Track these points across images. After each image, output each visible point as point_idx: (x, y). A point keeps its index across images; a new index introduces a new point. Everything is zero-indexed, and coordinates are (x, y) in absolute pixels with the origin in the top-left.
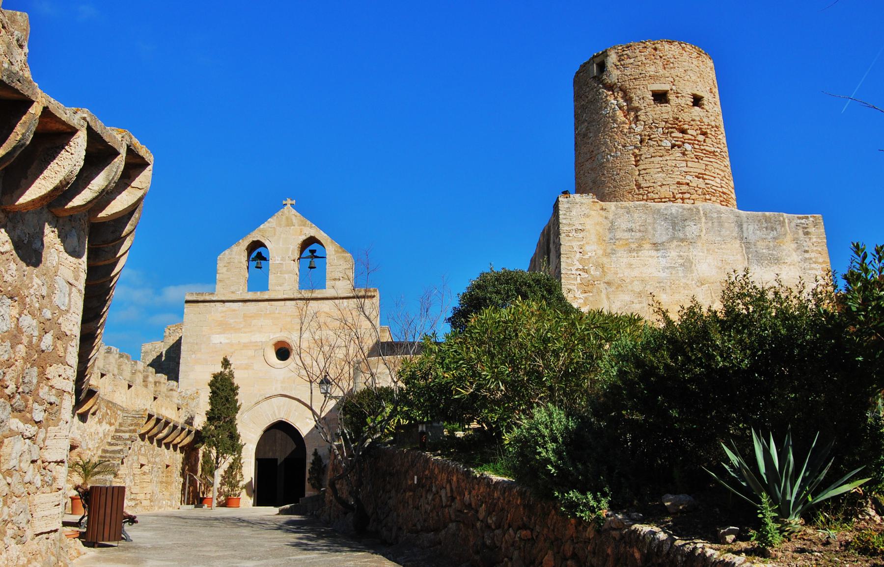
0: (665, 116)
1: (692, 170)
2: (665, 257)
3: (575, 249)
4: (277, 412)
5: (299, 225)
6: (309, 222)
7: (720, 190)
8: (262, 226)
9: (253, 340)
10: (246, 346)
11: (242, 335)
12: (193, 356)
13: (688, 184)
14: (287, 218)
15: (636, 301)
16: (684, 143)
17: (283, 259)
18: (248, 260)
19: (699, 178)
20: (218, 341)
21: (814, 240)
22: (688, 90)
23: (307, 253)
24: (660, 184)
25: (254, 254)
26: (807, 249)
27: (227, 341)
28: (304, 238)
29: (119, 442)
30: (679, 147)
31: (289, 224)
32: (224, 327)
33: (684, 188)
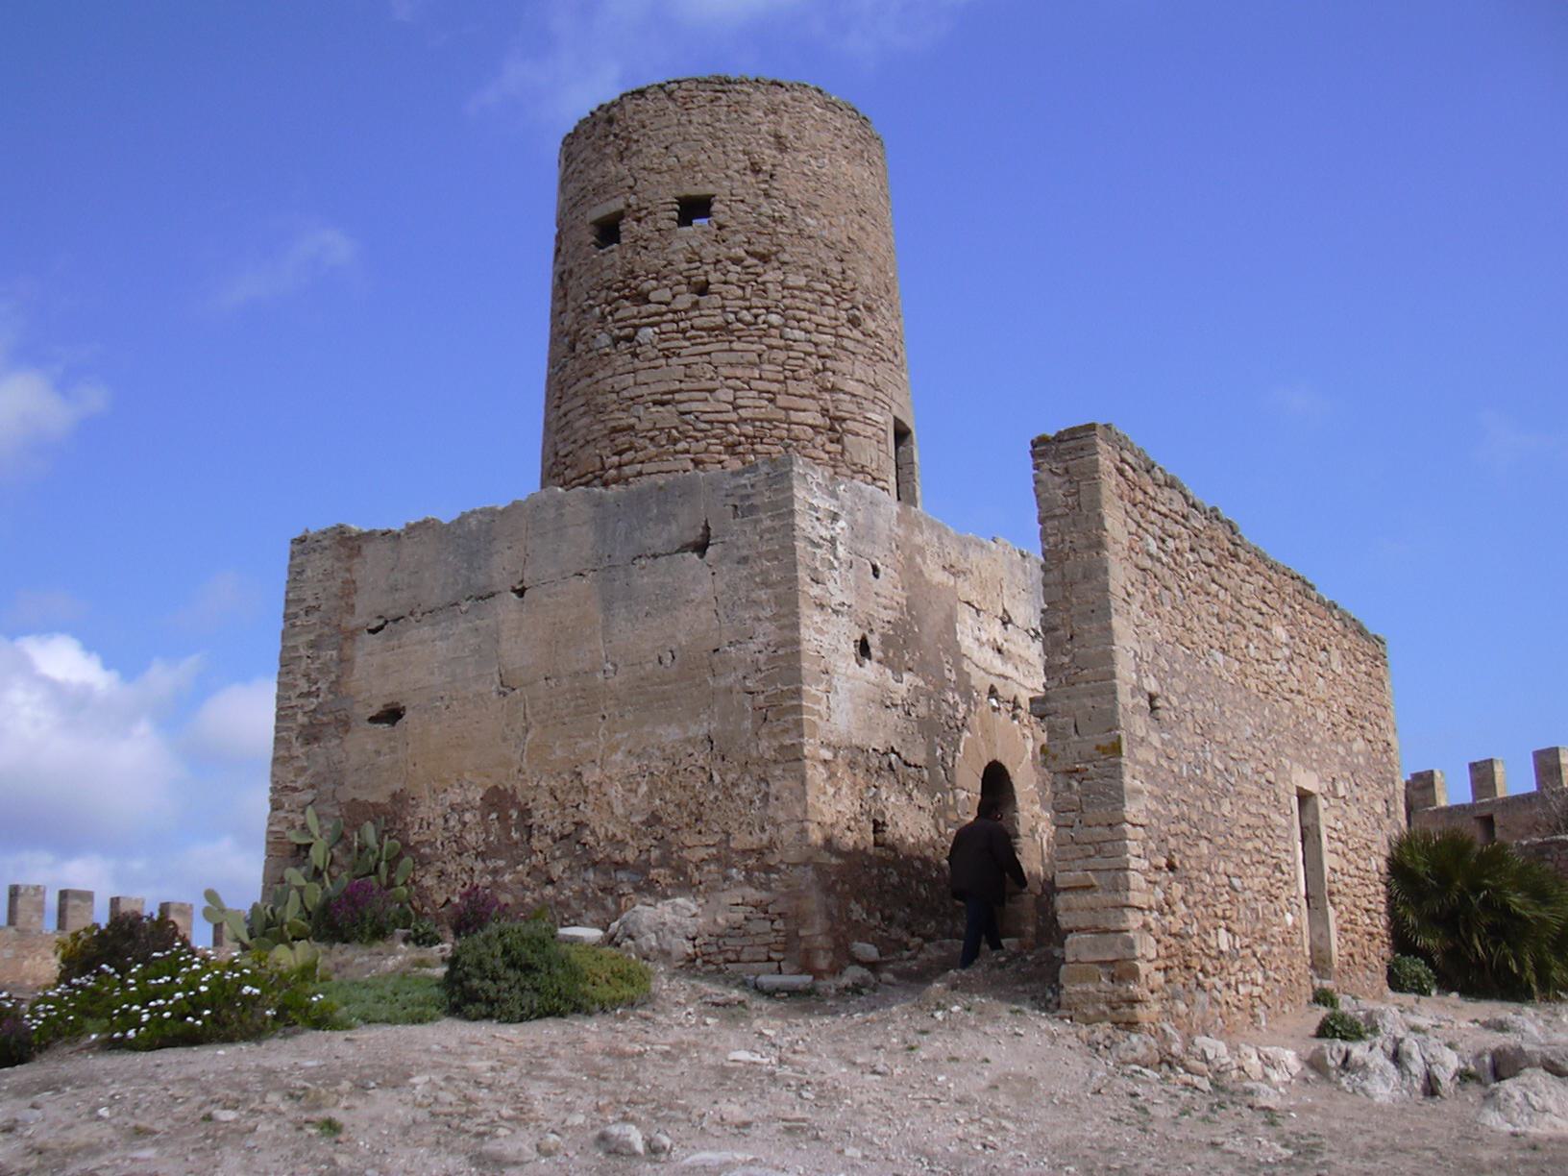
0: (608, 275)
1: (644, 390)
2: (444, 637)
3: (302, 652)
7: (734, 416)
13: (632, 427)
15: (385, 749)
16: (636, 327)
19: (663, 404)
21: (768, 523)
22: (664, 193)
24: (581, 442)
26: (745, 552)
30: (629, 339)
33: (622, 440)
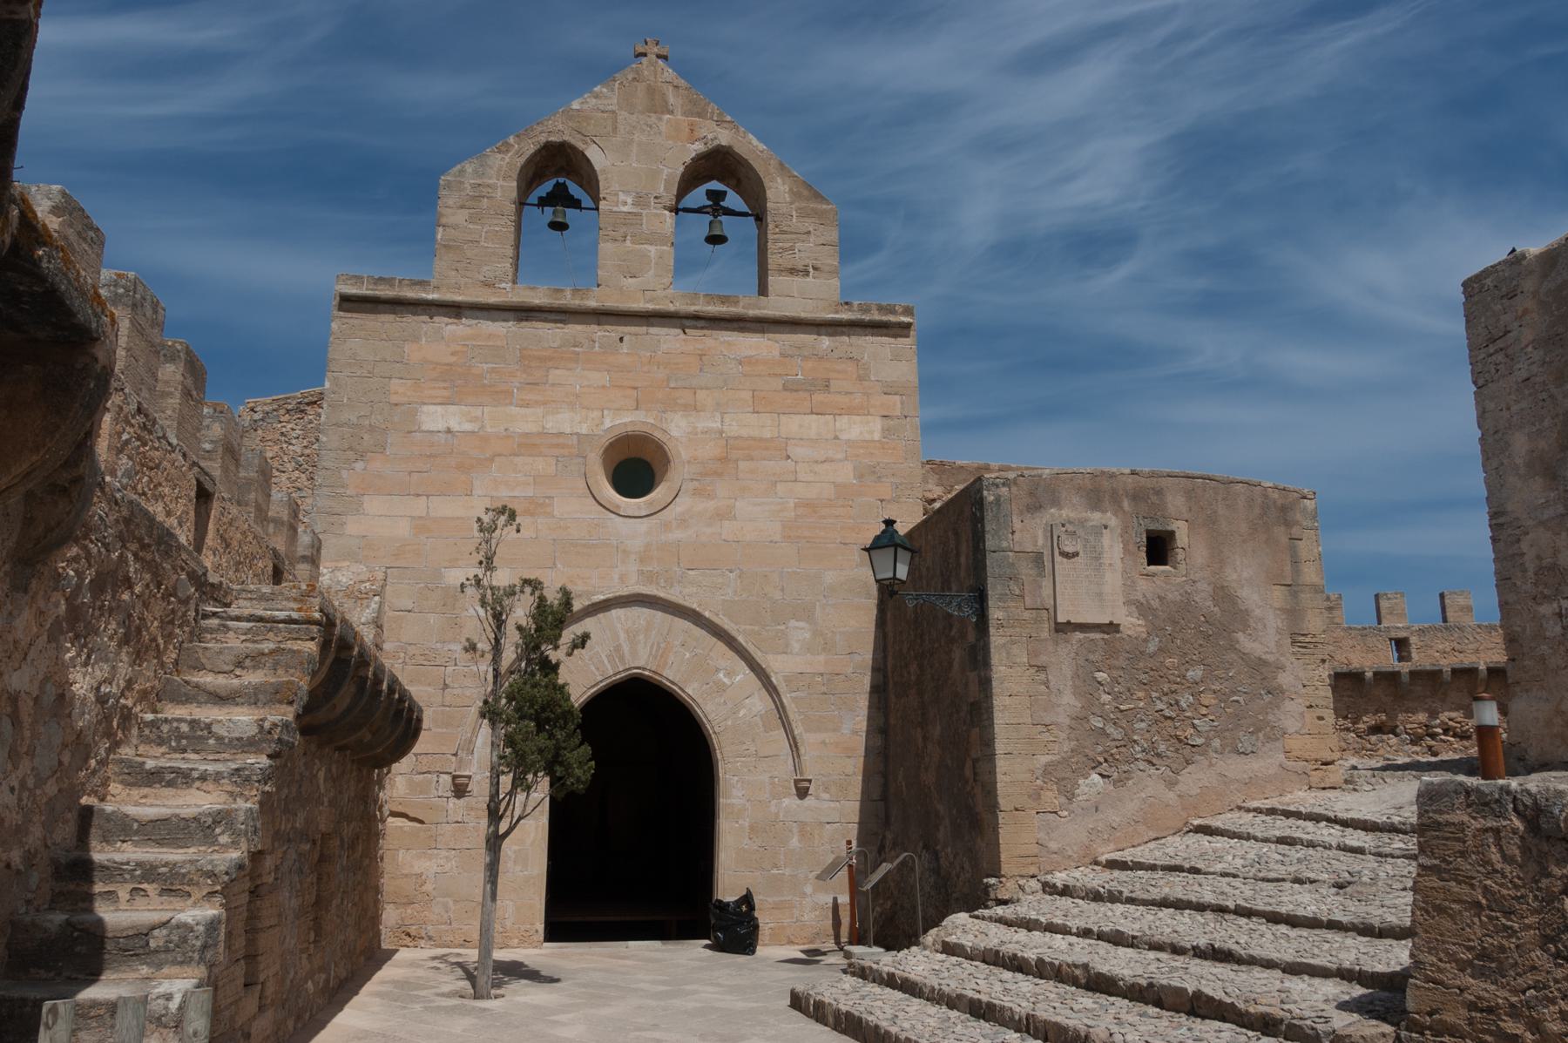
4: (626, 648)
5: (684, 114)
6: (712, 108)
8: (575, 105)
9: (551, 425)
10: (529, 445)
11: (514, 410)
12: (359, 466)
14: (651, 91)
17: (640, 200)
18: (521, 203)
20: (441, 426)
23: (698, 197)
25: (547, 187)
27: (468, 427)
28: (699, 147)
29: (192, 761)
31: (657, 105)
32: (458, 383)
